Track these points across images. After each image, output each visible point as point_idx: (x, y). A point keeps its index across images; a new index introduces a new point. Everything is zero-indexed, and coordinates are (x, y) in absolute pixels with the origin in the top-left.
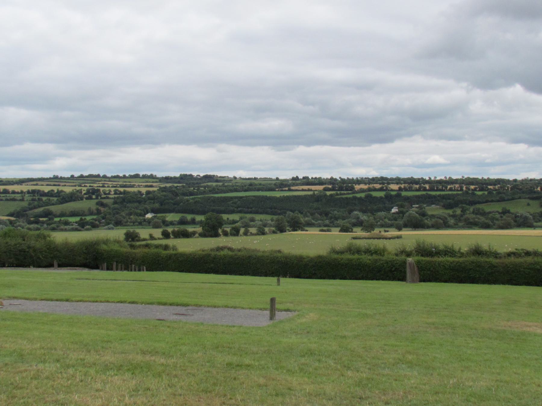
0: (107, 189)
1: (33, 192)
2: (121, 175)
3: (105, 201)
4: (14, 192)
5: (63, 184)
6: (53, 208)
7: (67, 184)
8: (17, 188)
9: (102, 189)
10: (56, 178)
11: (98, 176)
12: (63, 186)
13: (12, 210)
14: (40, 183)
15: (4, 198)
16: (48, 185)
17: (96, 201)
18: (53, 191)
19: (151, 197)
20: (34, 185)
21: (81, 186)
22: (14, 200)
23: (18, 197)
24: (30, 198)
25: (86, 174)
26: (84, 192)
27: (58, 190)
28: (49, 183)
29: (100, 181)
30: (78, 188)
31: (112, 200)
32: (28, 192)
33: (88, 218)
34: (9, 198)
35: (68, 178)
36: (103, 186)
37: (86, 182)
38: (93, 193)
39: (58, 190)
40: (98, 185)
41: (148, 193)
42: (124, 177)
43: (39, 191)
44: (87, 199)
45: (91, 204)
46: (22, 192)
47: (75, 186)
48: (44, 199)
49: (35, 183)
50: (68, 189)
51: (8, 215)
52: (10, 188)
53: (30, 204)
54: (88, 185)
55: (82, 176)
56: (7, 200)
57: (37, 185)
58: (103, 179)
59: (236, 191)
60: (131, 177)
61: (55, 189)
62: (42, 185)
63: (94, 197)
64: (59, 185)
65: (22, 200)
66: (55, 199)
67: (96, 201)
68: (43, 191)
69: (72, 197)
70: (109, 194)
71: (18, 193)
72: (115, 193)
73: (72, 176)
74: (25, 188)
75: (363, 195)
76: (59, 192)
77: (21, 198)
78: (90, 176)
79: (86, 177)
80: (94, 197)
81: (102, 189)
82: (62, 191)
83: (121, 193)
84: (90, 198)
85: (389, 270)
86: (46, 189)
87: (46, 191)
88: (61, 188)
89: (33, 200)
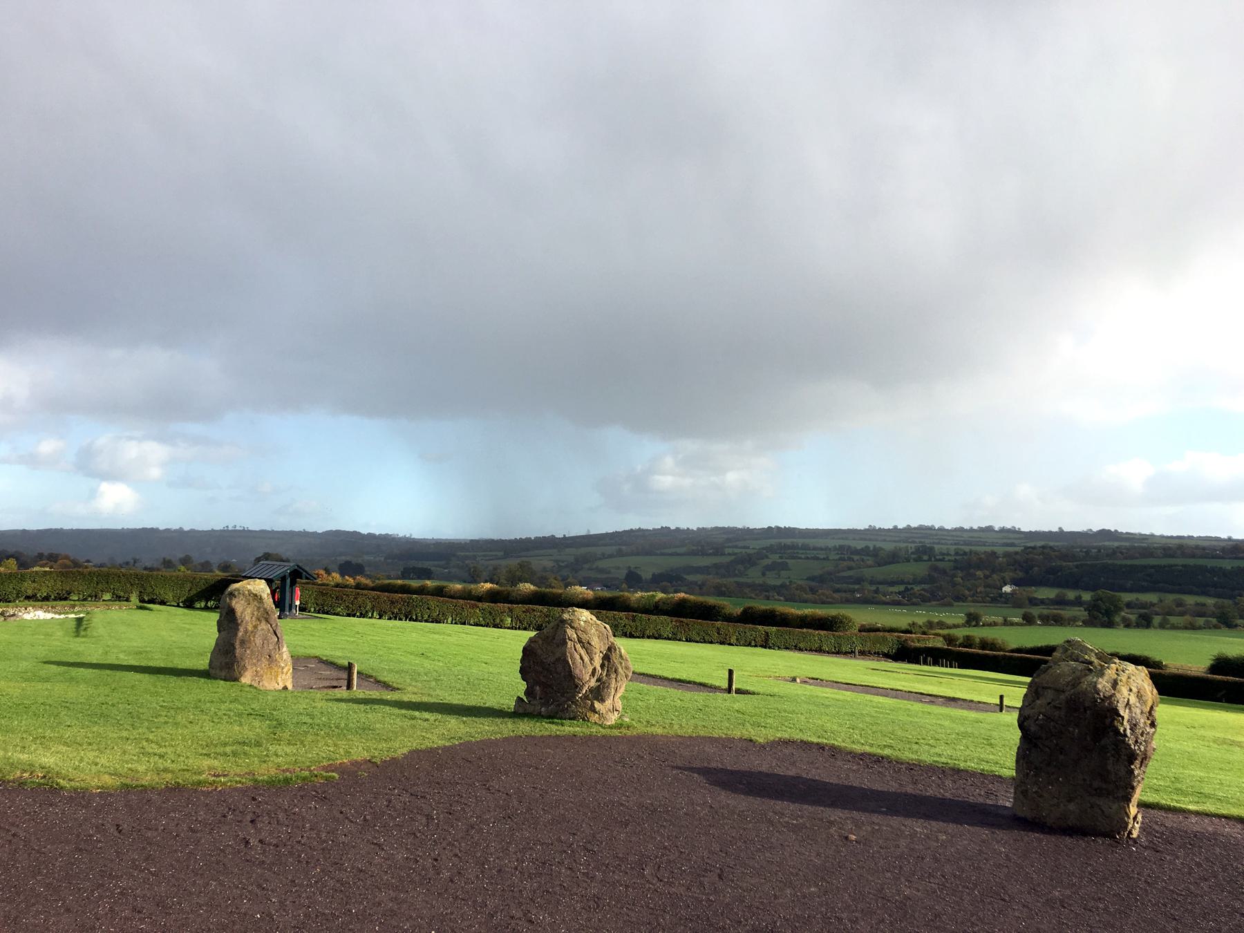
3: (941, 565)
4: (815, 549)
6: (868, 573)
9: (936, 547)
18: (867, 547)
32: (835, 548)
33: (917, 588)
38: (925, 553)
41: (1007, 555)
42: (972, 530)
44: (916, 560)
45: (920, 569)
69: (893, 558)
71: (821, 549)
72: (957, 554)
80: (925, 558)
82: (881, 549)
83: (965, 553)
84: (918, 560)
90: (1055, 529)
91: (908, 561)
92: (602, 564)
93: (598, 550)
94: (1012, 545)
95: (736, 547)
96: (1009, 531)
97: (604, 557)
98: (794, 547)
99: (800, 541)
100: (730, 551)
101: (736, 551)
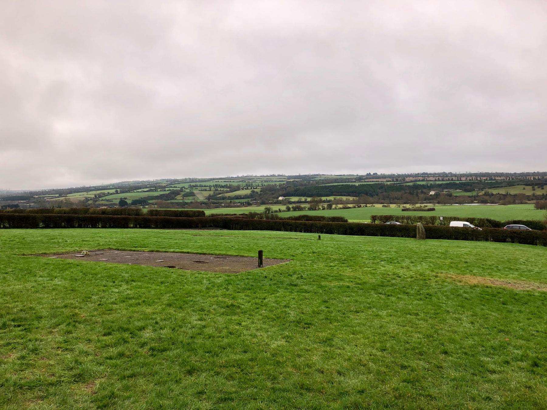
1: (216, 186)
2: (265, 175)
3: (255, 190)
4: (205, 186)
14: (220, 181)
19: (282, 188)
23: (208, 188)
31: (260, 190)
32: (214, 186)
41: (280, 185)
42: (267, 176)
45: (248, 192)
50: (235, 184)
59: (332, 183)
60: (271, 176)
65: (210, 190)
74: (211, 183)
75: (411, 184)
80: (250, 188)
85: (406, 231)
88: (231, 183)
90: (298, 174)
92: (108, 198)
93: (106, 192)
94: (282, 181)
96: (281, 176)
97: (109, 194)
99: (198, 184)
100: (168, 189)
101: (171, 189)
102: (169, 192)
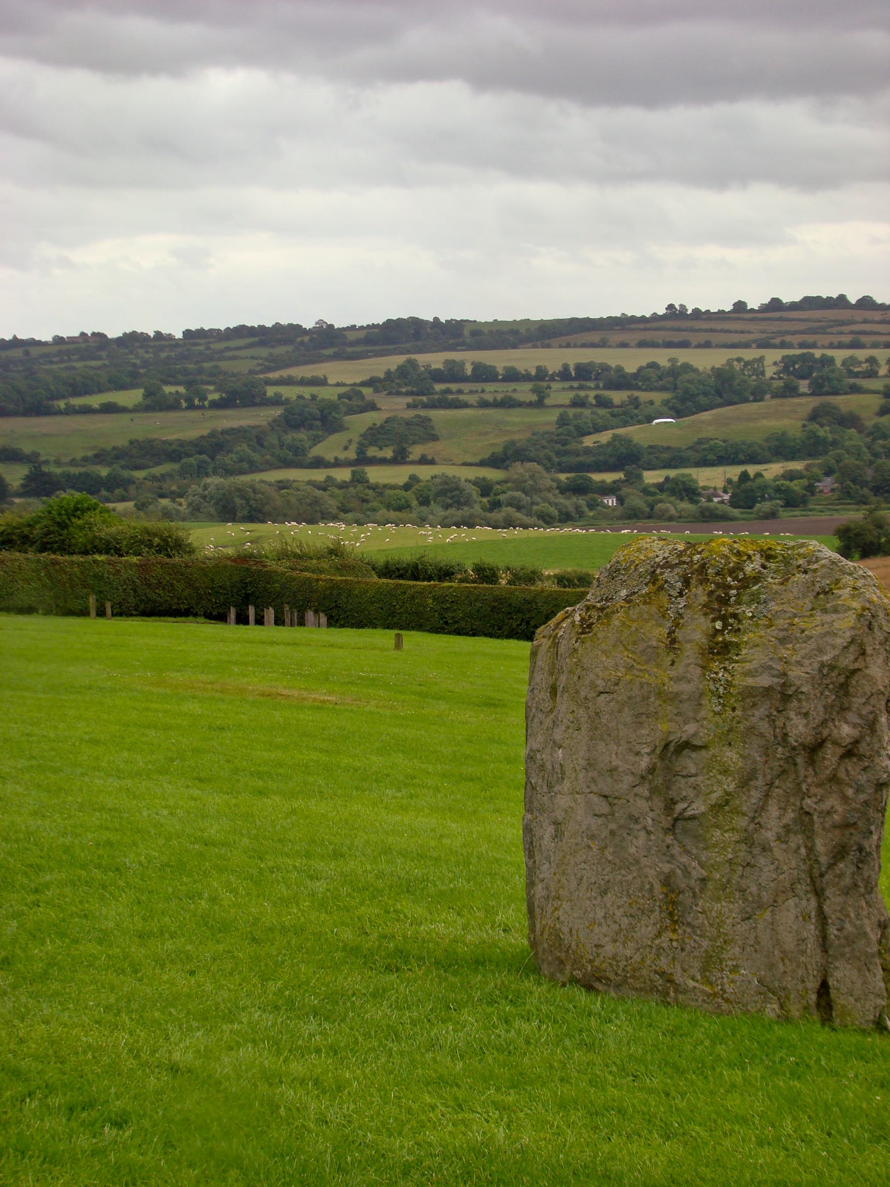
0: (861, 354)
1: (584, 373)
3: (844, 403)
4: (512, 376)
5: (701, 338)
7: (715, 338)
8: (526, 359)
10: (675, 314)
11: (841, 301)
12: (699, 346)
13: (496, 442)
15: (472, 399)
16: (642, 344)
17: (813, 402)
18: (653, 365)
20: (593, 345)
21: (765, 344)
22: (507, 404)
23: (524, 392)
24: (565, 398)
25: (790, 296)
26: (770, 372)
27: (673, 360)
28: (648, 336)
29: (843, 323)
30: (749, 355)
31: (875, 402)
32: (564, 375)
33: (773, 470)
34: (489, 398)
35: (721, 315)
36: (855, 345)
37: (785, 326)
39: (673, 360)
40: (836, 339)
43: (605, 368)
46: (541, 375)
47: (747, 346)
48: (618, 397)
49: (595, 337)
50: (706, 361)
51: (482, 464)
52: (499, 359)
53: (563, 421)
54: (796, 339)
55: (775, 305)
56: (484, 404)
57: (603, 344)
58: (859, 315)
61: (662, 357)
62: (624, 345)
63: (804, 386)
64: (684, 345)
65: (539, 404)
66: (658, 397)
67: (813, 402)
68: (620, 369)
70: (871, 374)
71: (527, 378)
73: (740, 306)
74: (554, 359)
76: (676, 371)
77: (534, 398)
78: (810, 303)
79: (794, 306)
81: (840, 355)
82: (687, 367)
84: (790, 391)
86: (631, 361)
87: (631, 368)
88: (683, 356)
89: (578, 403)
91: (758, 395)
95: (289, 382)
98: (452, 374)
99: (468, 359)
101: (289, 393)
102: (277, 412)
